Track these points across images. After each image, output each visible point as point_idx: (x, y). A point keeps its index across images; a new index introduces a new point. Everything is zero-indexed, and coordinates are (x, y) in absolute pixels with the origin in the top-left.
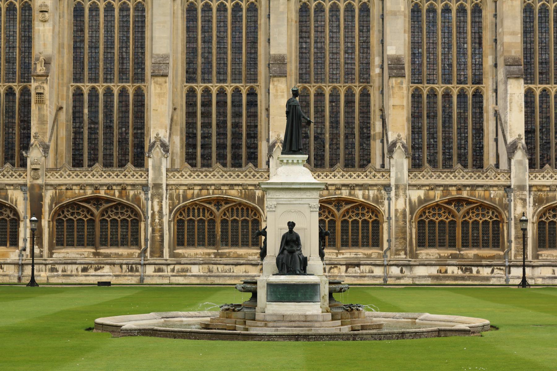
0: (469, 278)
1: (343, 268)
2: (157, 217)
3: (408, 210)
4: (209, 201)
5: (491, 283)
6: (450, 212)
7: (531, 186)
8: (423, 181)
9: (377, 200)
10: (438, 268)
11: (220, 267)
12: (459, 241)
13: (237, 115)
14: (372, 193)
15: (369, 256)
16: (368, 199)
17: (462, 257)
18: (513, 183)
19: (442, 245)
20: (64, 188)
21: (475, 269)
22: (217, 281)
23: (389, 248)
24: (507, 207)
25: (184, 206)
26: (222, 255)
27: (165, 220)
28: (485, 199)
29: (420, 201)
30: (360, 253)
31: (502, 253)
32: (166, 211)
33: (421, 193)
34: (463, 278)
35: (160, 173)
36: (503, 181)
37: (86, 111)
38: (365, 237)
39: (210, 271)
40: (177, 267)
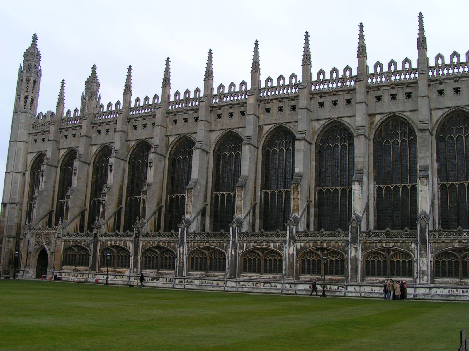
1: (262, 284)
15: (275, 278)
24: (347, 252)
39: (202, 283)
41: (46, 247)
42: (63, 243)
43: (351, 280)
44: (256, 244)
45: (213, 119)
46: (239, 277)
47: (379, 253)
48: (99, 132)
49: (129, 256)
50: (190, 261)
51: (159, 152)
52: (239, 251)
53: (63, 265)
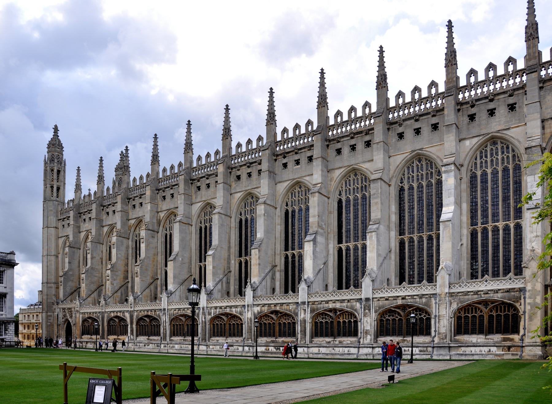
10: (265, 347)
15: (237, 341)
17: (276, 342)
24: (297, 314)
29: (258, 313)
39: (181, 347)
41: (70, 319)
42: (81, 316)
43: (300, 342)
44: (221, 310)
45: (193, 192)
46: (209, 341)
47: (326, 314)
48: (108, 213)
49: (127, 325)
50: (172, 328)
51: (151, 228)
52: (208, 318)
53: (82, 335)
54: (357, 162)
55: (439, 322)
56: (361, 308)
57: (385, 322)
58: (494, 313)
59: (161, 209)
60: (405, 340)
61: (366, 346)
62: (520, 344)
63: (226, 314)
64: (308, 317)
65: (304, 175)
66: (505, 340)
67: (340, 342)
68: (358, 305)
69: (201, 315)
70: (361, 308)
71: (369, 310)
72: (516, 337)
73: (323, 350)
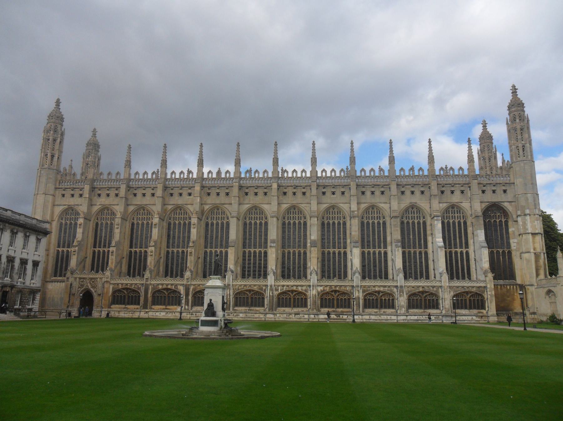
0: (339, 319)
1: (294, 315)
2: (228, 296)
3: (317, 294)
4: (247, 291)
5: (347, 321)
6: (332, 295)
7: (361, 286)
8: (322, 284)
9: (306, 291)
11: (250, 314)
12: (335, 306)
13: (260, 260)
14: (304, 288)
15: (303, 311)
16: (303, 290)
17: (337, 311)
18: (355, 285)
19: (329, 307)
20: (197, 285)
21: (341, 316)
22: (249, 319)
23: (310, 308)
24: (353, 293)
25: (238, 292)
26: (251, 310)
27: (231, 297)
28: (345, 290)
29: (321, 291)
30: (300, 309)
31: (351, 310)
32: (231, 294)
33: (322, 288)
34: (337, 319)
35: (230, 281)
36: (351, 284)
37: (208, 258)
38: (302, 304)
39: (246, 316)
40: (235, 314)
43: (356, 311)
44: (288, 288)
46: (275, 310)
52: (276, 293)
54: (376, 202)
55: (444, 302)
56: (398, 291)
57: (411, 300)
58: (472, 299)
59: (205, 202)
60: (425, 312)
61: (402, 314)
62: (486, 315)
63: (292, 291)
64: (361, 295)
65: (339, 202)
66: (479, 312)
67: (384, 312)
68: (395, 290)
69: (269, 291)
70: (398, 291)
71: (403, 293)
72: (484, 311)
73: (373, 317)
